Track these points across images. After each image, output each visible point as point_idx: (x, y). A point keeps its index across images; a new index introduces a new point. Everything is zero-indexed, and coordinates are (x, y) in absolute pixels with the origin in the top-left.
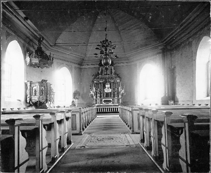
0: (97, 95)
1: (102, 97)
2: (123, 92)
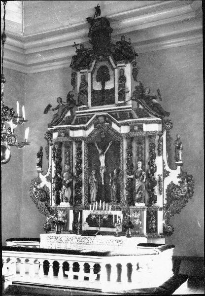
2: (176, 181)
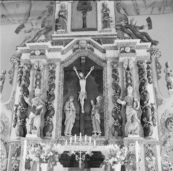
0: (24, 116)
1: (55, 132)
